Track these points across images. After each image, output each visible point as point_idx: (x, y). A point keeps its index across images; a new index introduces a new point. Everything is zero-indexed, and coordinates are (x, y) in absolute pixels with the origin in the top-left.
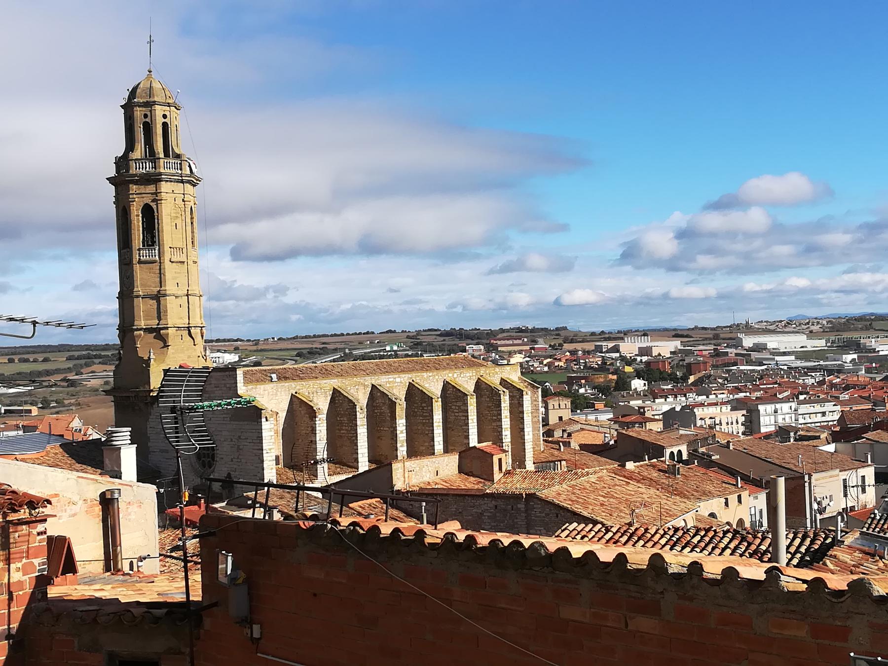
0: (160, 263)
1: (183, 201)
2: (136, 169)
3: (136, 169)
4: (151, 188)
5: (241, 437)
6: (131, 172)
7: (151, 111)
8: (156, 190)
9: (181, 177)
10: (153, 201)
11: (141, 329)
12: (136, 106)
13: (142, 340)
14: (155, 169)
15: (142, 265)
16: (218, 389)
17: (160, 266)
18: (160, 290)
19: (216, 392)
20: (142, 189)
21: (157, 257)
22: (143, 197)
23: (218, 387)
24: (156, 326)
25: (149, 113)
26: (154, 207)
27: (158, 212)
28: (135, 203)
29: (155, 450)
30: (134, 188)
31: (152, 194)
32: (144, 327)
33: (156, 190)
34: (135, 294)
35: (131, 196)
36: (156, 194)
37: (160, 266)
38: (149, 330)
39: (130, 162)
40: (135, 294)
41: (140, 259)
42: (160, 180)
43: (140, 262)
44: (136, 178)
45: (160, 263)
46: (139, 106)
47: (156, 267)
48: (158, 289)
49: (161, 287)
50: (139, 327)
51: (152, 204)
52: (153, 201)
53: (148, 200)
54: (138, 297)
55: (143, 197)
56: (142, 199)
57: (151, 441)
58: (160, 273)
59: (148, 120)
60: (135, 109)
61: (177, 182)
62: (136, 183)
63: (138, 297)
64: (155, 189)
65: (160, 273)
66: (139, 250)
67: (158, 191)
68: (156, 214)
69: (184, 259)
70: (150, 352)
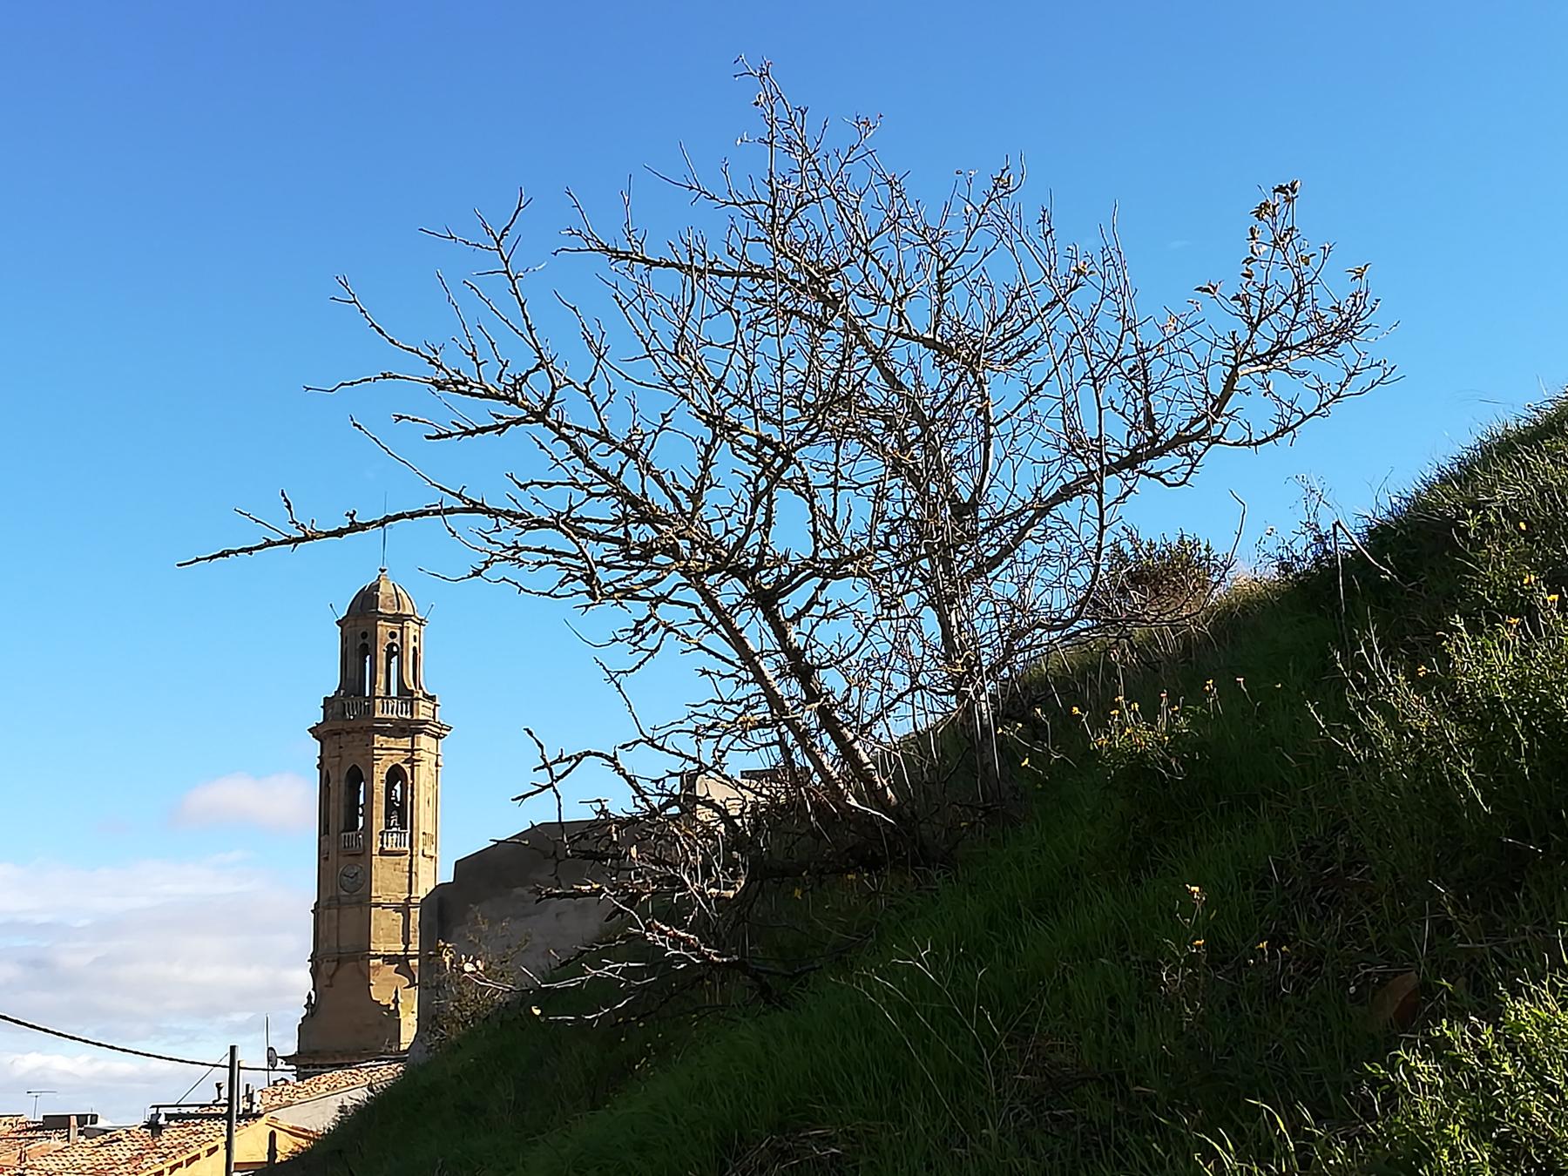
0: (412, 856)
1: (437, 765)
2: (383, 712)
3: (383, 712)
4: (405, 742)
6: (376, 716)
7: (401, 629)
8: (413, 745)
9: (441, 729)
10: (405, 762)
11: (378, 957)
12: (380, 619)
14: (412, 714)
15: (384, 857)
17: (411, 861)
18: (409, 898)
20: (392, 742)
21: (407, 848)
22: (392, 755)
24: (403, 953)
25: (398, 632)
26: (408, 771)
27: (412, 778)
28: (379, 762)
30: (379, 740)
31: (406, 751)
32: (386, 954)
33: (413, 745)
34: (373, 901)
35: (376, 752)
36: (412, 751)
37: (411, 861)
38: (389, 959)
39: (377, 700)
40: (373, 901)
41: (382, 848)
42: (421, 731)
43: (382, 852)
44: (389, 725)
45: (412, 856)
48: (407, 895)
49: (410, 892)
50: (379, 953)
51: (403, 766)
52: (405, 762)
53: (398, 760)
54: (378, 905)
55: (392, 755)
56: (390, 758)
58: (410, 871)
60: (379, 623)
61: (433, 736)
62: (383, 732)
63: (378, 905)
64: (410, 743)
65: (410, 871)
66: (382, 833)
67: (416, 747)
68: (410, 781)
69: (433, 854)
70: (396, 992)
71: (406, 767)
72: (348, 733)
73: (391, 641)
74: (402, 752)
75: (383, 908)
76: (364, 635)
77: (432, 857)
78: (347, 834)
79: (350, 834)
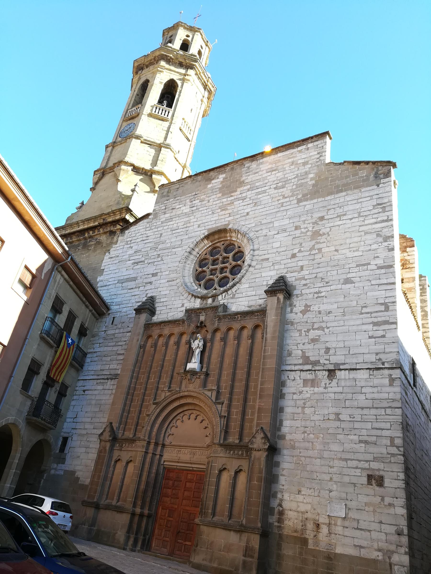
5: (326, 217)
10: (180, 79)
13: (127, 178)
16: (274, 172)
19: (268, 178)
23: (275, 170)
25: (191, 36)
29: (108, 284)
43: (150, 115)
44: (171, 55)
46: (185, 28)
47: (166, 124)
52: (180, 79)
54: (138, 137)
57: (104, 273)
59: (190, 39)
71: (179, 83)
72: (147, 67)
73: (186, 38)
74: (178, 74)
75: (142, 142)
76: (171, 36)
77: (189, 140)
78: (131, 110)
79: (133, 109)
